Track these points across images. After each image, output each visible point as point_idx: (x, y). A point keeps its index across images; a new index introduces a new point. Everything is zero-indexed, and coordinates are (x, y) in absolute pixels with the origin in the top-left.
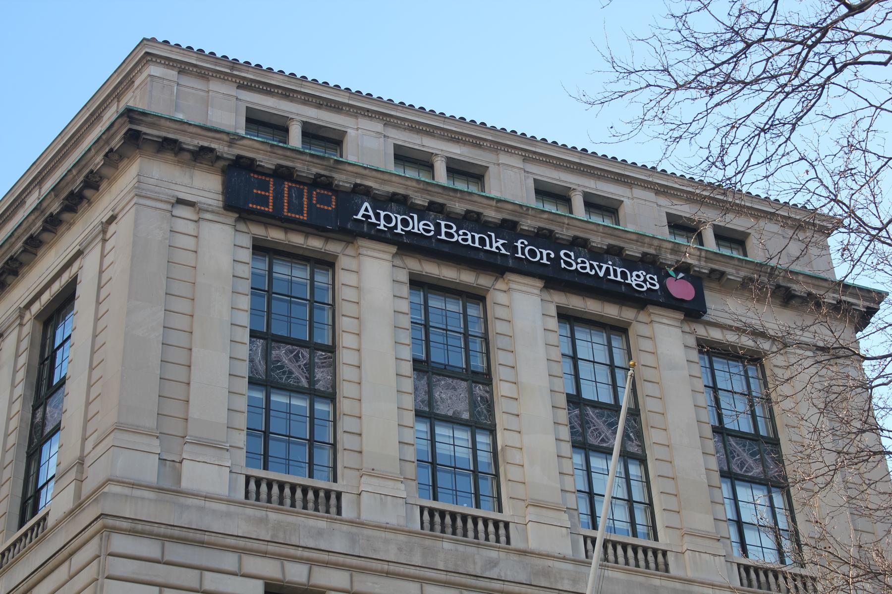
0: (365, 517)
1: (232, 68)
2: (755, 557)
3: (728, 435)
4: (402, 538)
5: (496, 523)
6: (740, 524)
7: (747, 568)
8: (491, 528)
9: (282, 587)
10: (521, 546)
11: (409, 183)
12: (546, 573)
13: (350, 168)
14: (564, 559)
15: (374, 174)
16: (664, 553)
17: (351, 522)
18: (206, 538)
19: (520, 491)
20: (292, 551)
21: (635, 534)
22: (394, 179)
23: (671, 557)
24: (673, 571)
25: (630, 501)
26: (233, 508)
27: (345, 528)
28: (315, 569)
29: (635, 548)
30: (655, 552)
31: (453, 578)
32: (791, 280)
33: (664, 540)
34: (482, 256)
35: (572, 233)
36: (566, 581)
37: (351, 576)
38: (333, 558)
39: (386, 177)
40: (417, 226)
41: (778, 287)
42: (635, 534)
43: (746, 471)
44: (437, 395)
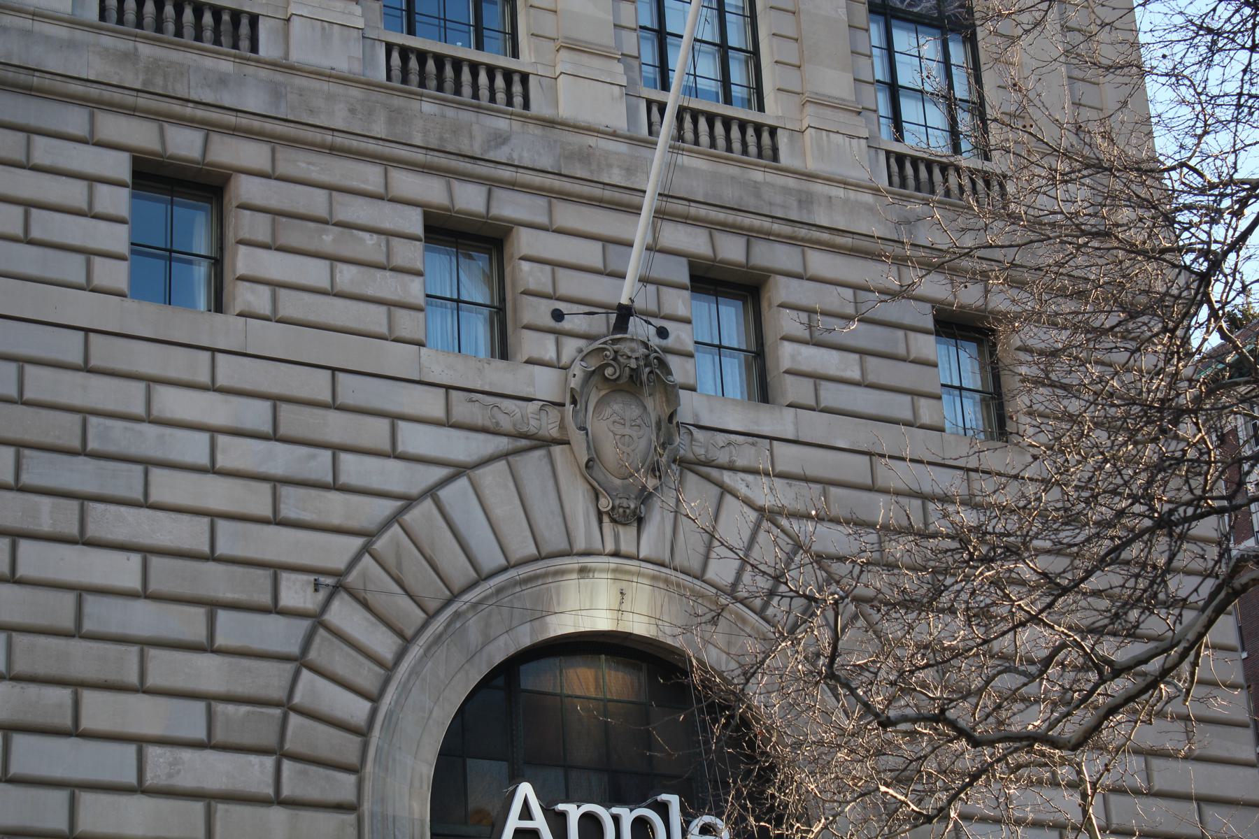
0: (296, 56)
2: (913, 142)
4: (355, 93)
5: (508, 75)
6: (894, 89)
7: (900, 158)
8: (500, 82)
9: (160, 164)
10: (547, 112)
12: (585, 157)
14: (614, 135)
16: (773, 131)
17: (274, 65)
18: (36, 80)
19: (548, 25)
20: (177, 108)
21: (728, 100)
23: (783, 139)
24: (785, 159)
25: (723, 48)
26: (79, 35)
27: (264, 73)
28: (215, 138)
29: (727, 122)
30: (758, 128)
31: (436, 159)
33: (774, 110)
36: (616, 171)
37: (273, 151)
38: (244, 121)
42: (728, 100)
43: (910, 5)
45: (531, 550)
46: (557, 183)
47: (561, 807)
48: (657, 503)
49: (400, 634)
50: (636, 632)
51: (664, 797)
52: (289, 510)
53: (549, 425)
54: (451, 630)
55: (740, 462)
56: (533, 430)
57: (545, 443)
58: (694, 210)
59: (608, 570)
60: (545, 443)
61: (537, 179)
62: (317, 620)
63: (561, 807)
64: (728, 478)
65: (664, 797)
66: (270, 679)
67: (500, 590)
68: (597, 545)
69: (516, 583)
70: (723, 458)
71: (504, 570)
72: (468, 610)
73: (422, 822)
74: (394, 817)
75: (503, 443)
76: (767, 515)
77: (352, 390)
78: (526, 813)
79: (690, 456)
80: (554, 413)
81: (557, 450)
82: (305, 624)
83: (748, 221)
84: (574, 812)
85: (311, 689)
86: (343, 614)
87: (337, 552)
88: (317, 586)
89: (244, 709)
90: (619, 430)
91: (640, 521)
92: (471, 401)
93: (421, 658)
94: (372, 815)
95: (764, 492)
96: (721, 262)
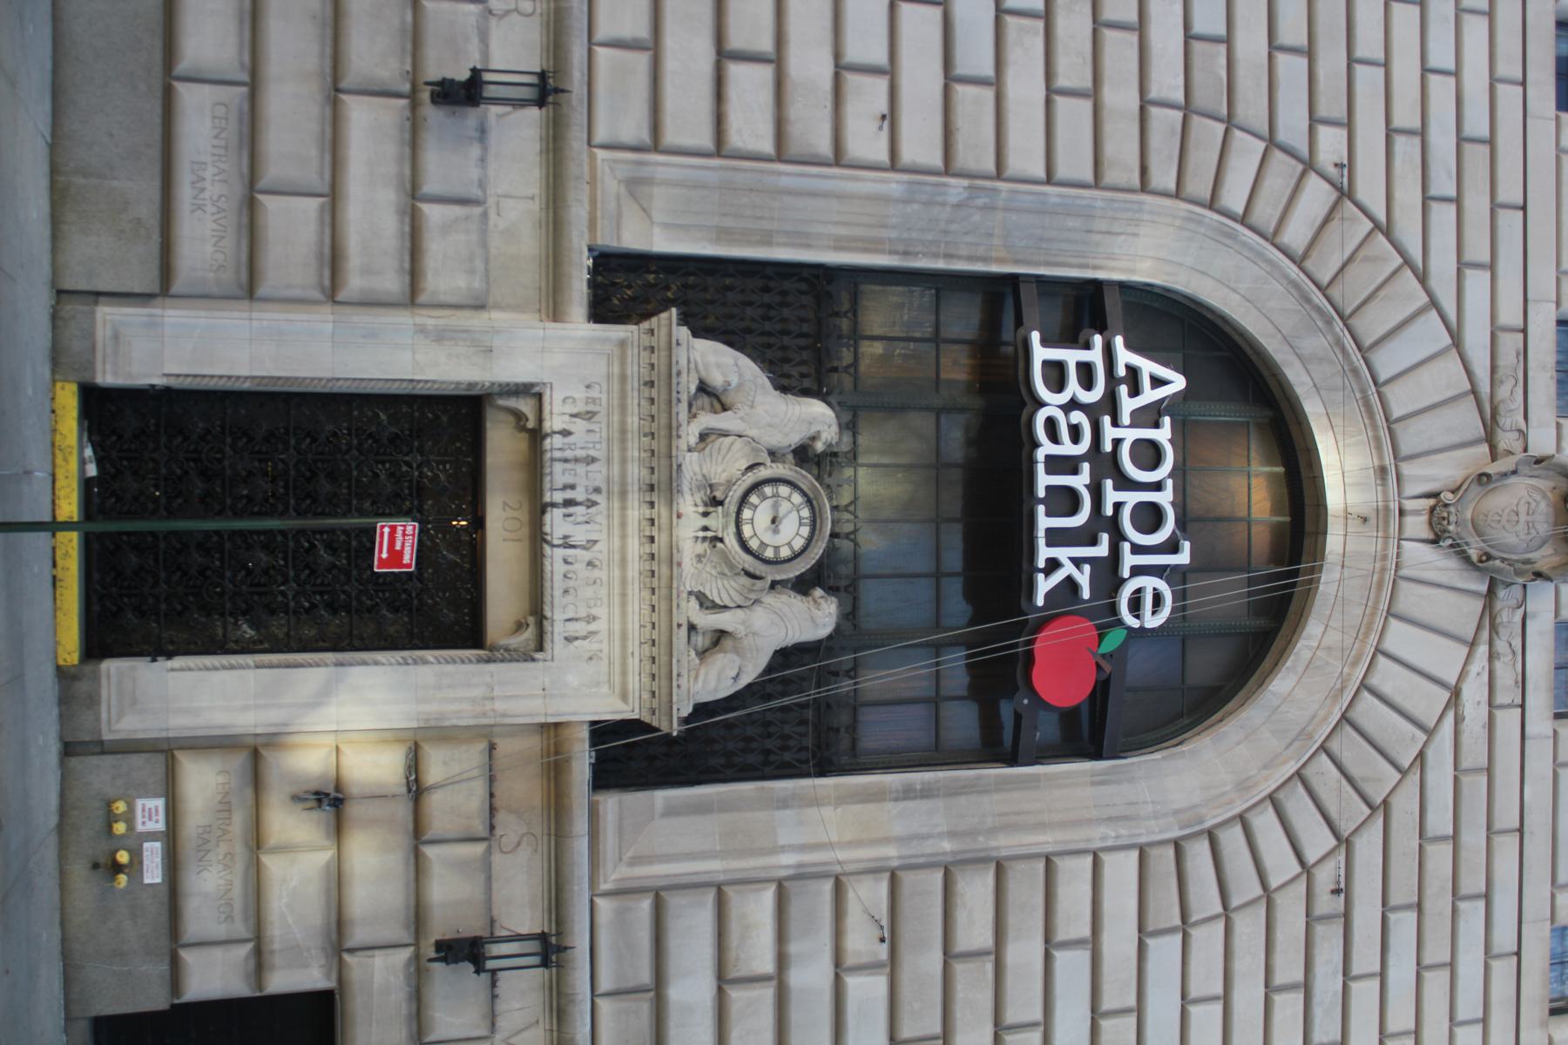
45: (1396, 413)
47: (1167, 420)
48: (1453, 563)
49: (1306, 255)
50: (1329, 538)
51: (1187, 545)
52: (1400, 142)
53: (1506, 440)
54: (1314, 315)
55: (1498, 665)
56: (1501, 421)
57: (1490, 438)
59: (1386, 500)
60: (1490, 438)
62: (1309, 165)
63: (1167, 420)
64: (1483, 649)
65: (1187, 545)
66: (1252, 108)
67: (1355, 372)
68: (1411, 489)
69: (1363, 391)
70: (1501, 646)
72: (1335, 334)
73: (1133, 271)
74: (1136, 235)
75: (1485, 388)
76: (1456, 693)
77: (1510, 222)
78: (1157, 382)
79: (1498, 605)
80: (1517, 446)
81: (1485, 448)
82: (1304, 150)
84: (1162, 434)
85: (1247, 151)
86: (1317, 195)
87: (1370, 190)
89: (1224, 74)
91: (1435, 542)
92: (1518, 354)
93: (1286, 277)
94: (1140, 203)
95: (1474, 694)
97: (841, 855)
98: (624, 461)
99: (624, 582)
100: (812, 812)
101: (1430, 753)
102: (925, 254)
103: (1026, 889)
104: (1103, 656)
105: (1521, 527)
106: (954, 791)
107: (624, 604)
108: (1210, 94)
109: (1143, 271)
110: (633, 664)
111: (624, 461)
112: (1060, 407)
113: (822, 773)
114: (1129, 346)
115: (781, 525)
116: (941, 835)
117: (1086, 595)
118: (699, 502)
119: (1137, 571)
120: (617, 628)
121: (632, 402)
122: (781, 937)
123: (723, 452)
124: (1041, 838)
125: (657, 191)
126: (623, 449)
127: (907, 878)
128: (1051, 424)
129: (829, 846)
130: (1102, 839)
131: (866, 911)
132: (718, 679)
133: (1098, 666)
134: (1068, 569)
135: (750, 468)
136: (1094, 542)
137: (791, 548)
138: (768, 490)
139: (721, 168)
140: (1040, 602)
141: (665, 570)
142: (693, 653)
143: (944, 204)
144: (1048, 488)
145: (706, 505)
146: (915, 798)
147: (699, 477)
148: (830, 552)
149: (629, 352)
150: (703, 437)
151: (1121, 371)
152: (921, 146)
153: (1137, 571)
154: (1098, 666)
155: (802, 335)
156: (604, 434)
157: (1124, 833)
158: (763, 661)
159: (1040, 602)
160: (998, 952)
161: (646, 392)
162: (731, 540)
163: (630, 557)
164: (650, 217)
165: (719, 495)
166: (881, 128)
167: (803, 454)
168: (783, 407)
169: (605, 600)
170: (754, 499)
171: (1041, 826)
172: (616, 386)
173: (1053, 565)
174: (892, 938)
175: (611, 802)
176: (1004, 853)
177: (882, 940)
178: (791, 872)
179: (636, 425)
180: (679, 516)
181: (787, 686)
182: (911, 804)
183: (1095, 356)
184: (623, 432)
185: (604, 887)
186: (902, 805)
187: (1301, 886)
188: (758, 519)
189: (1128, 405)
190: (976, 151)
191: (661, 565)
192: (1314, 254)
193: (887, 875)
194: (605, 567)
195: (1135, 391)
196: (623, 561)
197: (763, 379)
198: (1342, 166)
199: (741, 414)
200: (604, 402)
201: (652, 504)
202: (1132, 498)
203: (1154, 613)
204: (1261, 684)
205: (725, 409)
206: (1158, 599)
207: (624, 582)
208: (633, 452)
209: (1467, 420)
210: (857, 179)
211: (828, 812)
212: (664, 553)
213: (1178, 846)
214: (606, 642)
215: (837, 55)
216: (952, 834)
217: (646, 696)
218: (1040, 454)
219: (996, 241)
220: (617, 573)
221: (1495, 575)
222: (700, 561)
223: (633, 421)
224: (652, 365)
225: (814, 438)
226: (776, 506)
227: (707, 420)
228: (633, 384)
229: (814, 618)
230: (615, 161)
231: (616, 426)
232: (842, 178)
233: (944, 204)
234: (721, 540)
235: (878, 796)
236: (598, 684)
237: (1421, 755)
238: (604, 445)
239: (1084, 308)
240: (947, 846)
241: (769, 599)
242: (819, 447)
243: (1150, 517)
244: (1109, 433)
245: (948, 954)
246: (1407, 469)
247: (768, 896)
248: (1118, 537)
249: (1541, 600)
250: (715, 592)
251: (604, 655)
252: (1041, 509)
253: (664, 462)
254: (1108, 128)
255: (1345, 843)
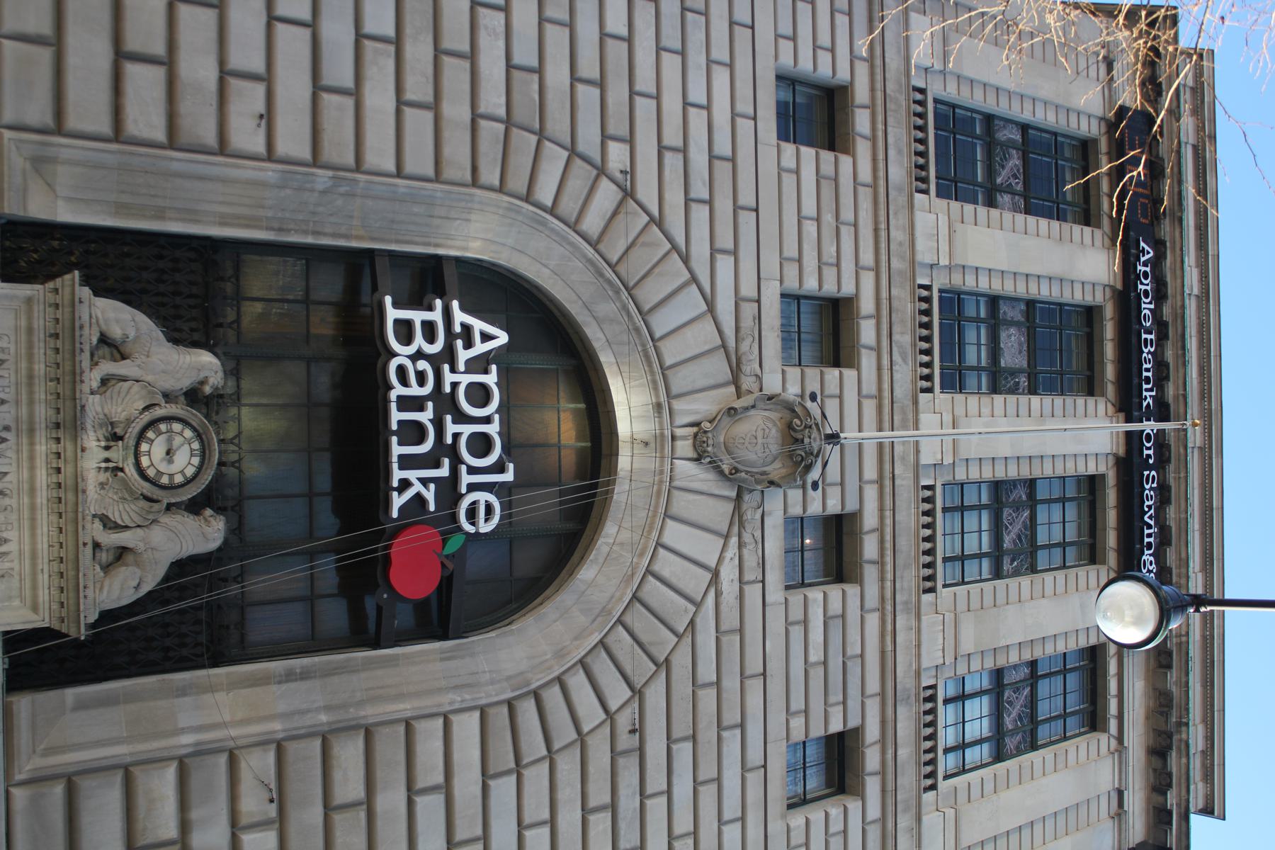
1: (1210, 137)
3: (1032, 686)
11: (1179, 298)
13: (1177, 234)
15: (1179, 260)
20: (880, 118)
22: (1179, 281)
32: (1179, 749)
34: (1136, 381)
35: (1172, 483)
38: (881, 165)
39: (1178, 272)
40: (1147, 306)
41: (1170, 736)
44: (1012, 330)
45: (668, 362)
46: (887, 402)
47: (494, 367)
48: (711, 476)
52: (669, 157)
53: (747, 382)
54: (606, 286)
55: (745, 552)
57: (736, 381)
58: (888, 514)
59: (662, 429)
60: (736, 381)
61: (886, 386)
62: (602, 170)
63: (494, 367)
64: (734, 540)
65: (511, 466)
66: (558, 124)
67: (637, 330)
68: (680, 420)
69: (644, 345)
70: (747, 537)
71: (653, 340)
72: (621, 301)
75: (731, 343)
76: (716, 574)
77: (747, 219)
78: (486, 337)
79: (744, 507)
80: (755, 387)
81: (732, 389)
82: (597, 158)
83: (889, 559)
84: (491, 379)
85: (555, 159)
86: (607, 195)
87: (647, 191)
88: (623, 172)
89: (536, 97)
90: (757, 436)
91: (698, 459)
93: (585, 256)
95: (728, 574)
96: (861, 539)
97: (234, 732)
98: (31, 402)
99: (33, 508)
100: (208, 698)
101: (698, 620)
102: (296, 231)
103: (390, 748)
104: (447, 556)
105: (759, 446)
106: (328, 673)
107: (33, 528)
108: (526, 112)
109: (474, 249)
110: (43, 579)
111: (31, 402)
112: (408, 357)
113: (215, 665)
114: (463, 309)
115: (175, 457)
116: (318, 710)
117: (432, 508)
118: (101, 437)
119: (472, 487)
120: (27, 548)
121: (39, 351)
122: (184, 805)
123: (122, 395)
124: (401, 706)
125: (60, 169)
126: (31, 393)
127: (292, 748)
128: (401, 370)
129: (224, 725)
130: (450, 704)
131: (257, 778)
132: (120, 589)
133: (443, 565)
134: (417, 487)
135: (147, 408)
136: (437, 465)
137: (184, 475)
138: (163, 427)
139: (120, 152)
140: (395, 514)
141: (71, 496)
142: (98, 568)
143: (312, 190)
144: (400, 422)
145: (107, 440)
146: (296, 680)
147: (101, 416)
148: (218, 477)
149: (36, 308)
150: (104, 382)
151: (458, 329)
152: (293, 141)
153: (472, 487)
154: (443, 565)
155: (191, 296)
156: (13, 379)
157: (468, 697)
158: (161, 572)
159: (395, 514)
160: (369, 802)
161: (52, 343)
162: (130, 470)
163: (38, 485)
164: (54, 191)
165: (119, 431)
166: (259, 125)
167: (193, 396)
168: (176, 357)
169: (16, 525)
170: (150, 434)
171: (400, 697)
172: (23, 337)
173: (405, 484)
174: (280, 799)
175: (24, 703)
176: (371, 721)
177: (272, 801)
178: (191, 750)
179: (42, 372)
180: (83, 450)
181: (183, 592)
182: (293, 685)
183: (436, 316)
184: (31, 377)
185: (19, 777)
186: (284, 687)
187: (607, 729)
188: (154, 452)
189: (463, 355)
190: (339, 147)
191: (67, 493)
192: (606, 238)
193: (274, 746)
194: (15, 496)
195: (468, 345)
196: (32, 490)
197: (158, 333)
198: (626, 173)
199: (138, 362)
200: (12, 351)
201: (58, 440)
202: (467, 430)
203: (486, 520)
204: (571, 574)
205: (124, 357)
206: (489, 509)
207: (33, 508)
208: (40, 394)
209: (718, 368)
210: (238, 167)
211: (221, 696)
212: (70, 482)
213: (510, 704)
214: (16, 562)
215: (222, 62)
216: (328, 708)
217: (55, 606)
218: (393, 395)
219: (355, 223)
220: (26, 500)
221: (741, 484)
222: (103, 488)
223: (39, 368)
224: (57, 320)
225: (202, 383)
226: (170, 440)
227: (107, 367)
228: (39, 335)
229: (207, 533)
230: (21, 141)
231: (24, 372)
232: (226, 165)
233: (312, 190)
234: (122, 470)
235: (264, 680)
236: (10, 598)
237: (692, 623)
238: (13, 389)
239: (428, 278)
240: (323, 718)
241: (165, 519)
242: (207, 390)
243: (481, 444)
244: (449, 378)
245: (328, 808)
246: (677, 405)
247: (171, 772)
248: (456, 461)
249: (774, 502)
250: (117, 514)
251: (15, 573)
252: (394, 439)
253: (68, 403)
254: (446, 134)
255: (638, 693)
